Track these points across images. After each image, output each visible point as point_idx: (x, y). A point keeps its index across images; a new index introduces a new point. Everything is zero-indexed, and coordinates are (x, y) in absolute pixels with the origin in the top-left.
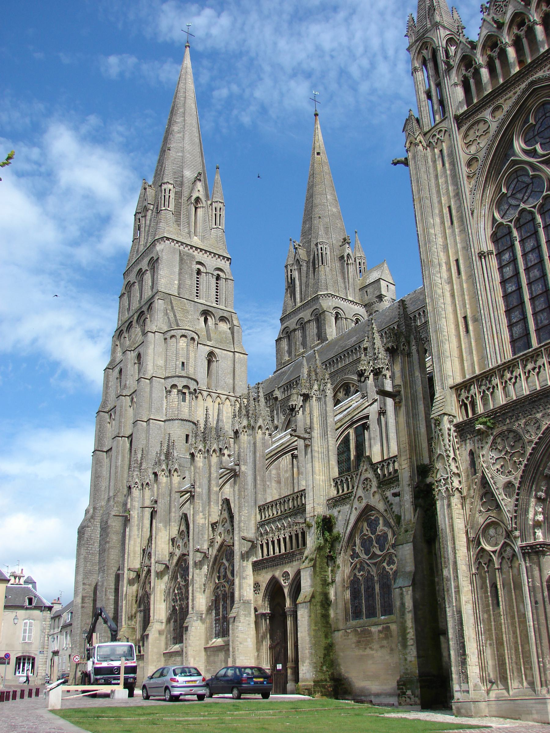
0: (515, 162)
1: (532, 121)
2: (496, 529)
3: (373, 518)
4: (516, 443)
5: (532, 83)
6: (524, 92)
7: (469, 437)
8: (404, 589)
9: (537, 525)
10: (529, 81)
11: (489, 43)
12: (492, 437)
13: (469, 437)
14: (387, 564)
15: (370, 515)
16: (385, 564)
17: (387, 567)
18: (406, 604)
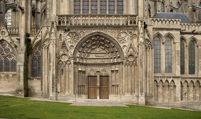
4: (76, 36)
7: (60, 30)
9: (78, 57)
12: (68, 33)
13: (60, 30)
18: (21, 70)
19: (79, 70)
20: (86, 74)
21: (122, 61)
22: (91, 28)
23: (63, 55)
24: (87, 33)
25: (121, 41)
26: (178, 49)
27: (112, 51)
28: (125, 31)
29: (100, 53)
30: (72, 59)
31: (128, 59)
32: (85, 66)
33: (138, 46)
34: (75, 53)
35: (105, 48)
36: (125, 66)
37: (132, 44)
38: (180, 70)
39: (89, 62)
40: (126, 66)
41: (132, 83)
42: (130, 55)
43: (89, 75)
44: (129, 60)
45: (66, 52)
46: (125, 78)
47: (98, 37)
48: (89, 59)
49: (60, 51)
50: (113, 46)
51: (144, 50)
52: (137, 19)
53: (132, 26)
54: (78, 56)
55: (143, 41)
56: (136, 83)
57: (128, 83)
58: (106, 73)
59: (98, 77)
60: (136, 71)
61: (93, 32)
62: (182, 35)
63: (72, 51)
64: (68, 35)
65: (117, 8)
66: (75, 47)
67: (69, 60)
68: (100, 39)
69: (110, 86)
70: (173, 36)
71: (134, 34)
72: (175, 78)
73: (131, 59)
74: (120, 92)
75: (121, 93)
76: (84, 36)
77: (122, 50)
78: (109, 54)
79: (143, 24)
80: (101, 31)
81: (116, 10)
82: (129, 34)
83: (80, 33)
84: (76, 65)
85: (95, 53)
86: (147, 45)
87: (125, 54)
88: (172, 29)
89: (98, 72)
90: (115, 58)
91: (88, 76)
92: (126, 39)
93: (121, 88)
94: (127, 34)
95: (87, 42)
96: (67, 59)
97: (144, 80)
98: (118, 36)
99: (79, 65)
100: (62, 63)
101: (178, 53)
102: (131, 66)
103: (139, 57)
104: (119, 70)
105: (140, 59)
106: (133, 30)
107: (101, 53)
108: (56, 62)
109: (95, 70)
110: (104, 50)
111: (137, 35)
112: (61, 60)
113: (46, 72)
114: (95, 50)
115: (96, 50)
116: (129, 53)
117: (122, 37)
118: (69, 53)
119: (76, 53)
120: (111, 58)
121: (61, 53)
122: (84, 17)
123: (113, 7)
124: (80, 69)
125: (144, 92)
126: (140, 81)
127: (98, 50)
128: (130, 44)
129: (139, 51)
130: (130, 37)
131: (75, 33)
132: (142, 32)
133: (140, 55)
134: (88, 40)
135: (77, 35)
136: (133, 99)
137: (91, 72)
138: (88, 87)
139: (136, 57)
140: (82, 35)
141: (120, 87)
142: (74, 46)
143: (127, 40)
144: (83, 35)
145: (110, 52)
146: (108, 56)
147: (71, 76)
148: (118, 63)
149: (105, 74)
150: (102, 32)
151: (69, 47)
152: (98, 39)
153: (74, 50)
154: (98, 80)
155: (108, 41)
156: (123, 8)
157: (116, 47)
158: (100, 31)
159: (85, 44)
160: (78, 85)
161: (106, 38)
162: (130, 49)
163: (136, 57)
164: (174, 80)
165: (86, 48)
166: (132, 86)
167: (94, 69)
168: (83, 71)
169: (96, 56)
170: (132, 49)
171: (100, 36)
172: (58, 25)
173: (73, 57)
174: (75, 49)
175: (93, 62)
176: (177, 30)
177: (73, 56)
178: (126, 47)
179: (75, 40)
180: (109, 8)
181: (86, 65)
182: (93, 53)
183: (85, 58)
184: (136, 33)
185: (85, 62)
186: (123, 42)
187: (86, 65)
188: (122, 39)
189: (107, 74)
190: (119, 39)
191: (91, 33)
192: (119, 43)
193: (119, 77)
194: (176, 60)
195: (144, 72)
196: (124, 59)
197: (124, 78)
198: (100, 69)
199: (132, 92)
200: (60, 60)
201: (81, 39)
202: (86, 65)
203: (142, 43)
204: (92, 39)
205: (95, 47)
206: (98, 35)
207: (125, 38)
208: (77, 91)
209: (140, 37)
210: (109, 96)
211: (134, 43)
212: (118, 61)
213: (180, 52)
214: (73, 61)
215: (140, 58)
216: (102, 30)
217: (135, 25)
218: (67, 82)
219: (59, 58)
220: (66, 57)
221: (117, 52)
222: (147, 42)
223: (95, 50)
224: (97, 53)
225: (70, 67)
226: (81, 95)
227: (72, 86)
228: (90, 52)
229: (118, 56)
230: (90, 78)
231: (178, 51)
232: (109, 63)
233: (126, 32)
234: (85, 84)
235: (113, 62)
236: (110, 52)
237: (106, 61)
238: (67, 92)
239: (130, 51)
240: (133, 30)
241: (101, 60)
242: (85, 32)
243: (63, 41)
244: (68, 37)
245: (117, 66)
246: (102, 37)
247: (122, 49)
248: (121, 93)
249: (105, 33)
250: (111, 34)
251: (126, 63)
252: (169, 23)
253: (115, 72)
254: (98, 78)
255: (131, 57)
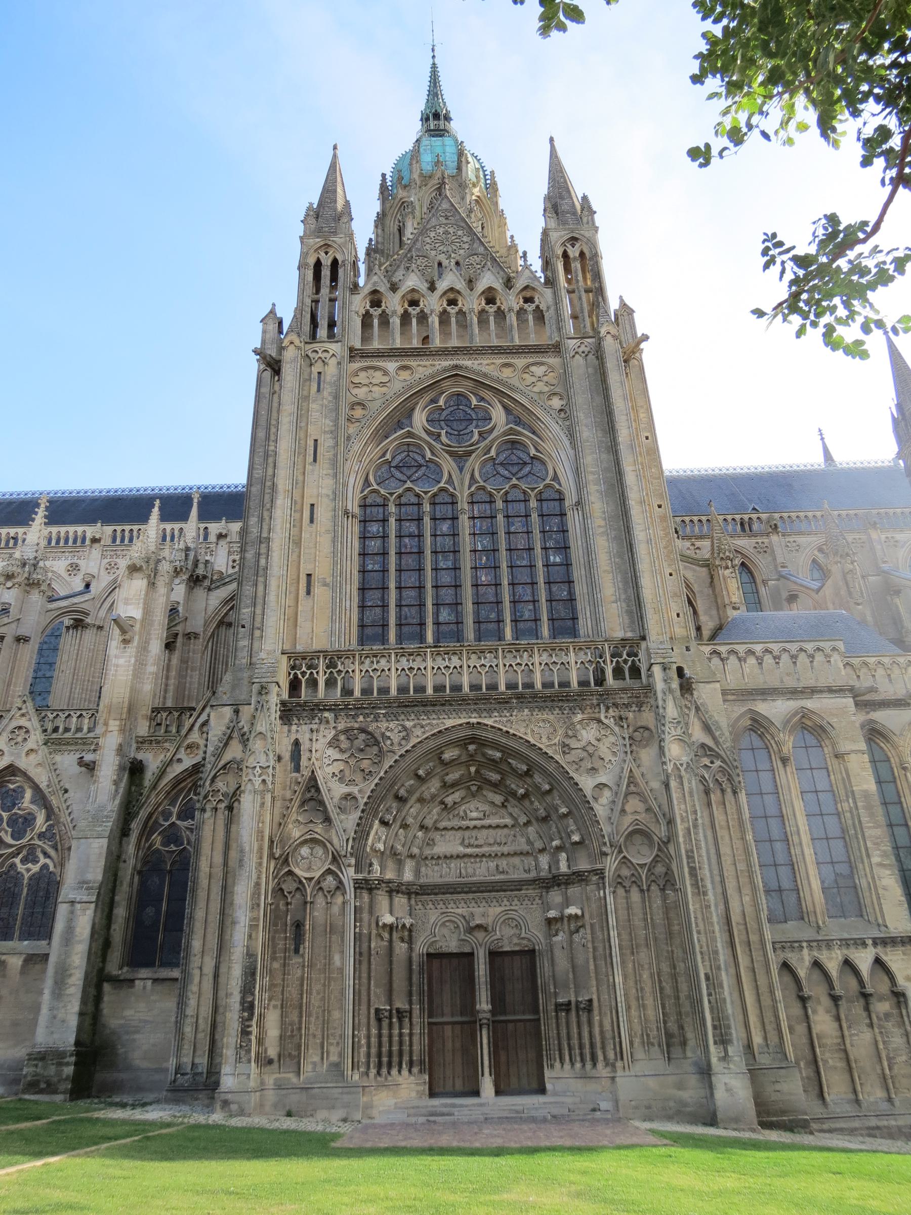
0: (410, 435)
1: (441, 402)
2: (312, 849)
3: (12, 786)
5: (456, 367)
6: (445, 370)
8: (78, 906)
10: (455, 362)
11: (409, 297)
13: (296, 721)
14: (22, 861)
15: (8, 781)
16: (17, 860)
17: (19, 865)
18: (78, 930)
19: (385, 925)
20: (419, 944)
21: (599, 866)
22: (437, 708)
23: (305, 842)
24: (418, 732)
25: (582, 764)
26: (865, 787)
27: (542, 813)
28: (597, 715)
29: (483, 827)
30: (349, 866)
31: (625, 854)
32: (413, 902)
33: (667, 785)
34: (362, 832)
35: (506, 800)
36: (614, 892)
37: (637, 773)
38: (903, 899)
39: (433, 875)
40: (621, 891)
41: (661, 989)
42: (630, 829)
43: (431, 951)
44: (634, 861)
45: (319, 828)
46: (623, 962)
47: (471, 747)
48: (432, 858)
49: (290, 826)
50: (547, 787)
51: (697, 803)
52: (642, 655)
53: (624, 690)
54: (380, 846)
55: (685, 759)
56: (684, 987)
57: (642, 989)
58: (523, 935)
59: (482, 961)
60: (672, 915)
61: (449, 723)
62: (868, 713)
63: (350, 821)
64: (330, 744)
65: (551, 610)
66: (362, 801)
67: (332, 868)
68: (479, 758)
69: (546, 1011)
70: (824, 723)
71: (639, 724)
72: (889, 949)
73: (642, 856)
74: (603, 1048)
75: (611, 1055)
76: (408, 748)
77: (592, 809)
78: (531, 829)
79: (675, 676)
80: (486, 721)
81: (545, 618)
82: (617, 729)
83: (388, 734)
84: (366, 896)
85: (460, 828)
86: (706, 776)
87: (606, 829)
88: (813, 691)
89: (479, 927)
90: (559, 849)
91: (429, 955)
92: (604, 750)
93: (607, 1026)
94: (608, 727)
95: (421, 772)
96: (326, 867)
97: (723, 966)
98: (567, 741)
99: (380, 892)
100: (298, 889)
101: (869, 807)
102: (645, 888)
103: (681, 840)
104: (587, 916)
105: (687, 852)
106: (634, 708)
107: (490, 827)
108: (267, 883)
109: (464, 917)
110: (503, 811)
111: (653, 728)
112: (293, 869)
113: (209, 937)
114: (462, 813)
115: (465, 811)
116: (628, 820)
117: (583, 743)
118: (334, 831)
119: (368, 834)
120: (542, 851)
121: (296, 833)
122: (404, 659)
123: (531, 607)
124: (388, 919)
125: (735, 1042)
126: (702, 976)
127: (474, 810)
128: (626, 774)
129: (676, 807)
130: (621, 741)
131: (363, 730)
132: (676, 715)
133: (680, 828)
134: (429, 761)
135: (373, 741)
136: (680, 1086)
137: (445, 931)
138: (429, 1023)
139: (663, 842)
140: (396, 740)
141: (600, 1014)
142: (358, 796)
143: (608, 756)
144: (403, 742)
145: (533, 820)
146: (524, 840)
147: (342, 958)
148: (578, 877)
149: (516, 941)
150: (489, 722)
151: (336, 800)
152: (471, 756)
153: (359, 814)
154: (483, 979)
155: (519, 766)
156: (574, 610)
157: (561, 797)
158: (479, 720)
159: (412, 782)
160: (377, 1011)
161: (508, 752)
162: (630, 798)
163: (663, 842)
164: (885, 958)
165: (418, 805)
166: (663, 1007)
167: (459, 911)
168: (404, 926)
169: (466, 842)
170: (638, 798)
171: (482, 743)
172: (285, 696)
173: (352, 854)
174: (363, 811)
175: (448, 874)
176: (835, 691)
177: (352, 847)
178: (607, 793)
179: (362, 767)
180: (514, 612)
181: (417, 892)
182: (453, 828)
183: (412, 856)
184: (647, 718)
185: (408, 876)
186: (593, 769)
187: (417, 894)
188: (585, 754)
189: (525, 942)
190: (573, 752)
191: (440, 732)
192: (572, 774)
193: (591, 955)
194: (869, 844)
195: (715, 919)
196: (606, 854)
197: (616, 959)
198: (489, 912)
199: (668, 1046)
200: (290, 873)
201: (391, 763)
202: (417, 892)
203: (682, 769)
204: (447, 756)
205: (457, 796)
206: (473, 740)
207: (600, 745)
208: (369, 1046)
209: (668, 738)
210: (547, 1073)
211: (643, 769)
212: (575, 869)
213: (876, 800)
214: (351, 871)
215: (682, 846)
216: (490, 712)
217: (635, 684)
218: (318, 993)
219: (286, 862)
220: (319, 851)
221: (565, 816)
222: (706, 761)
223: (462, 813)
224: (468, 828)
225: (336, 909)
226: (394, 1071)
227: (344, 1017)
228: (435, 822)
229: (576, 838)
230: (436, 963)
231: (866, 795)
232: (533, 875)
233: (603, 718)
234: (410, 1003)
235: (554, 871)
236: (533, 820)
237: (517, 870)
238: (317, 1059)
239: (628, 808)
240: (634, 708)
241: (492, 865)
242: (409, 724)
243: (305, 773)
244: (334, 754)
245: (574, 891)
246: (493, 748)
247: (588, 802)
248: (611, 1055)
249: (505, 729)
250: (533, 729)
251: (619, 876)
252: (795, 663)
253: (566, 927)
254: (482, 967)
255: (638, 839)
